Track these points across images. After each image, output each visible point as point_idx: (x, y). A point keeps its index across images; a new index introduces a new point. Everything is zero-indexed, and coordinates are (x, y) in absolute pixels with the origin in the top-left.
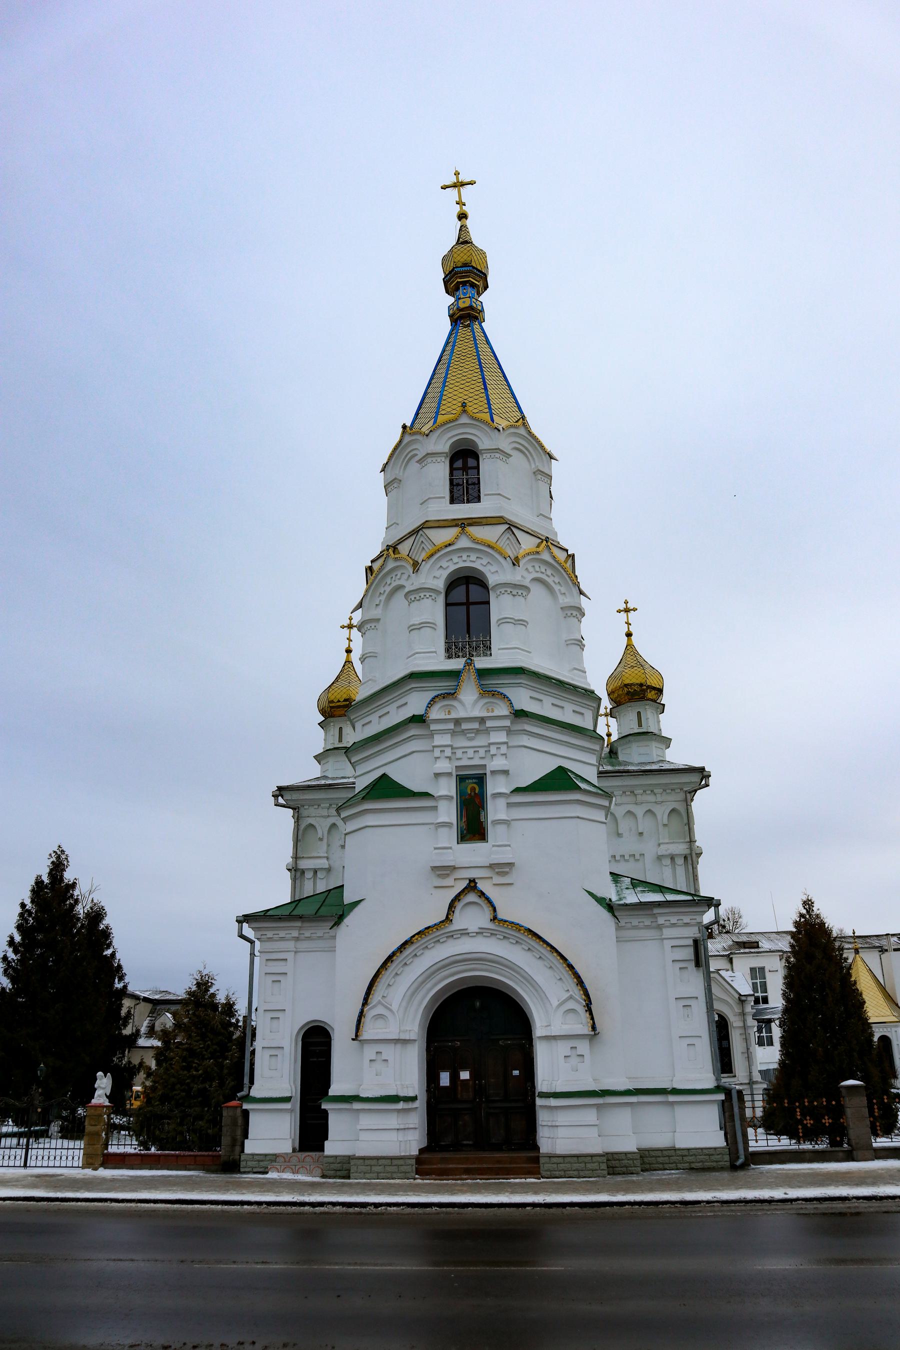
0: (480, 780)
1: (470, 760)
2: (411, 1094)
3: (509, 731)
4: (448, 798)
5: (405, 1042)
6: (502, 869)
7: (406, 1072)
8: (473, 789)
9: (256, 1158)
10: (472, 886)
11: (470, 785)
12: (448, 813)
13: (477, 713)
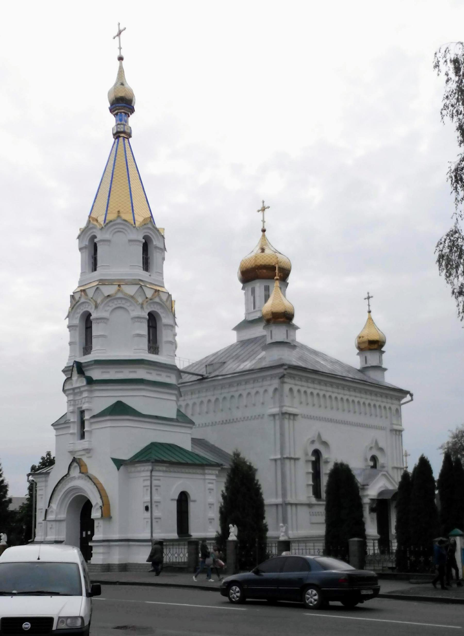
2: (62, 540)
3: (90, 391)
4: (74, 422)
5: (60, 521)
6: (88, 451)
10: (74, 460)
12: (75, 429)
13: (78, 385)
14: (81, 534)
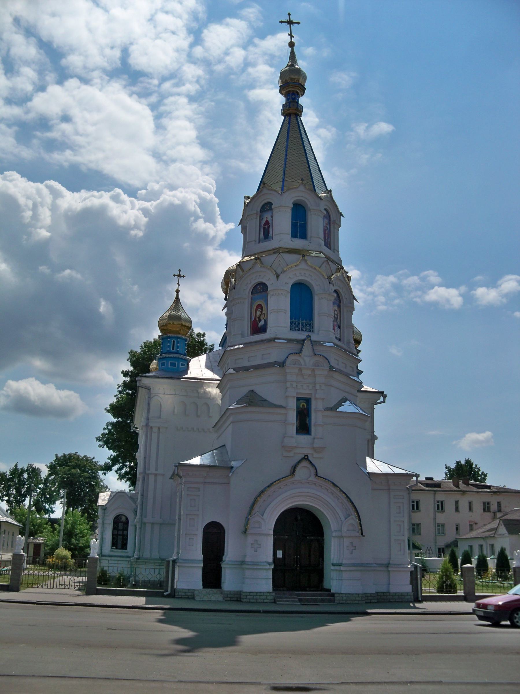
0: (308, 401)
1: (305, 392)
7: (266, 551)
8: (303, 406)
9: (183, 591)
11: (303, 404)
12: (292, 417)
14: (275, 554)
